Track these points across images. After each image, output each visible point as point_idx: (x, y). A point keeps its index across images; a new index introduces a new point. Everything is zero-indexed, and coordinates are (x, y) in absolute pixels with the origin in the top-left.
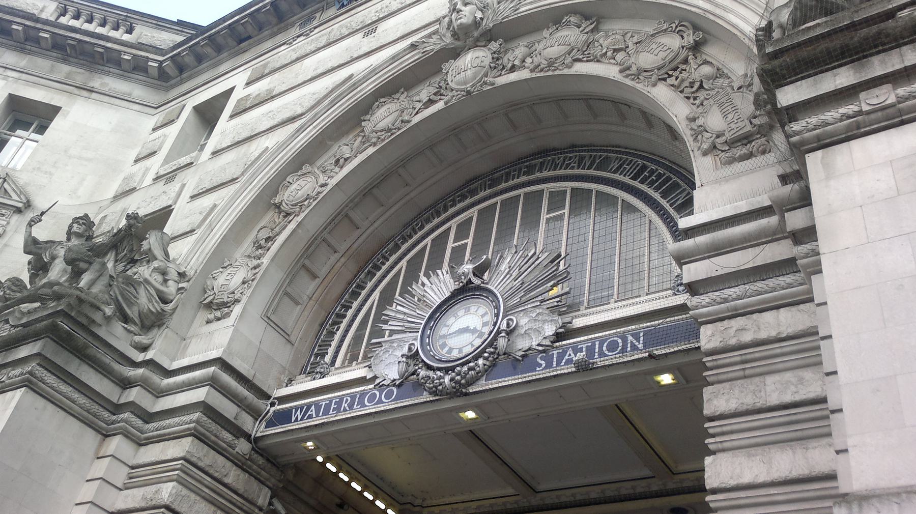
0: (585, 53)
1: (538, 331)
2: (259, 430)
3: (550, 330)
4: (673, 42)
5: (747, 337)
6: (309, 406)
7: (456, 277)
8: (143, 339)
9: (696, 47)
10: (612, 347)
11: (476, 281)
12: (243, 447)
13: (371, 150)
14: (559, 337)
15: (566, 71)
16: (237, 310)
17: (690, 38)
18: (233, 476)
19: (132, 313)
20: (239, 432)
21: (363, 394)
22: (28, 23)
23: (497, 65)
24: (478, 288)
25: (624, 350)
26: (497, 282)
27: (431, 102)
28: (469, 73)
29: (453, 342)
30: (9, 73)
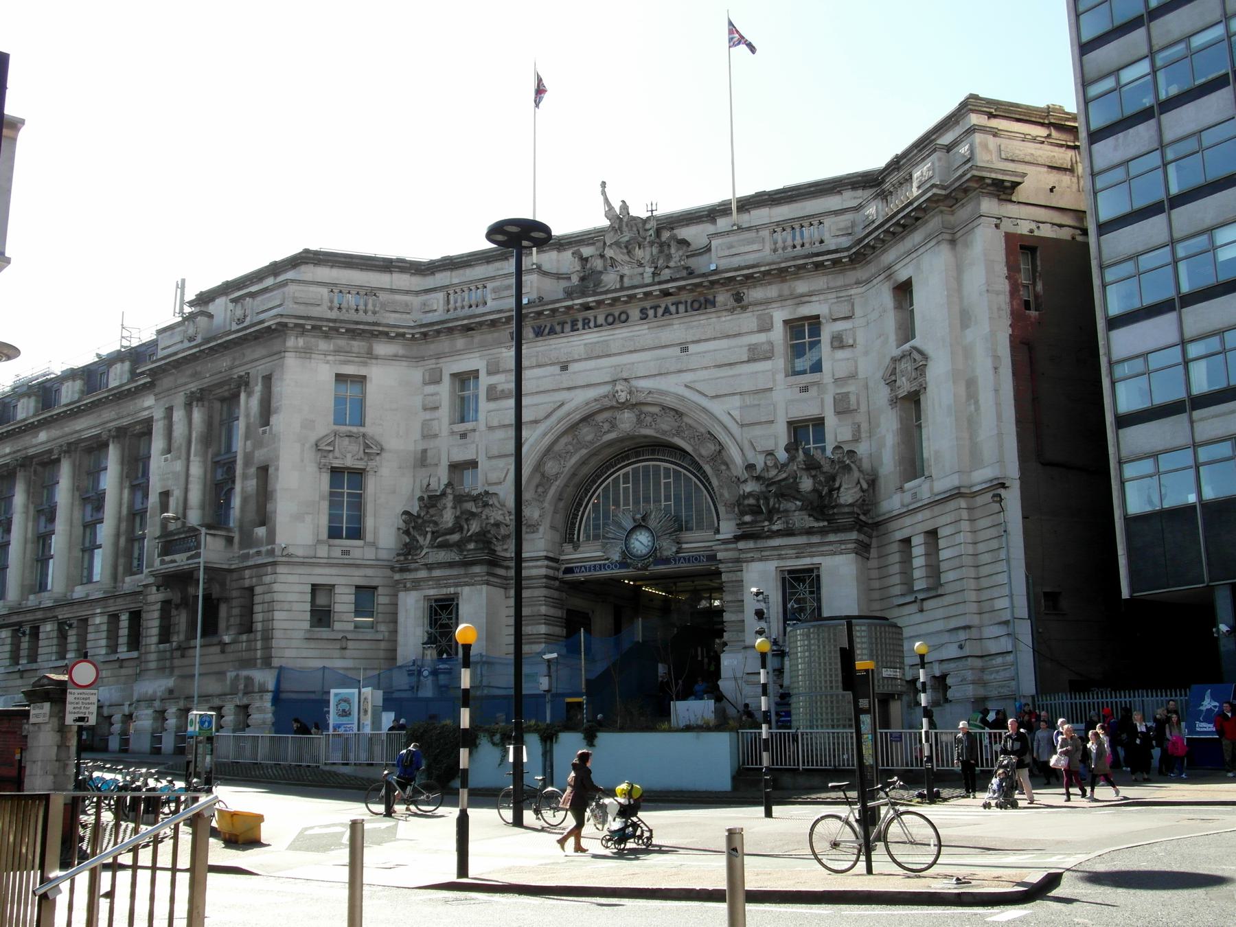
0: (679, 432)
1: (670, 549)
2: (560, 575)
3: (674, 549)
4: (713, 448)
5: (734, 579)
6: (581, 567)
7: (635, 520)
8: (505, 547)
9: (720, 451)
10: (696, 559)
11: (643, 524)
12: (557, 583)
13: (584, 451)
14: (677, 552)
15: (670, 439)
16: (541, 529)
17: (718, 448)
18: (556, 594)
19: (499, 537)
20: (555, 579)
21: (605, 565)
22: (331, 324)
23: (639, 421)
24: (644, 526)
25: (700, 561)
26: (652, 523)
27: (609, 432)
28: (628, 425)
29: (637, 544)
30: (330, 358)
